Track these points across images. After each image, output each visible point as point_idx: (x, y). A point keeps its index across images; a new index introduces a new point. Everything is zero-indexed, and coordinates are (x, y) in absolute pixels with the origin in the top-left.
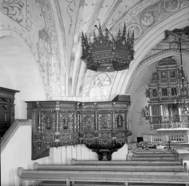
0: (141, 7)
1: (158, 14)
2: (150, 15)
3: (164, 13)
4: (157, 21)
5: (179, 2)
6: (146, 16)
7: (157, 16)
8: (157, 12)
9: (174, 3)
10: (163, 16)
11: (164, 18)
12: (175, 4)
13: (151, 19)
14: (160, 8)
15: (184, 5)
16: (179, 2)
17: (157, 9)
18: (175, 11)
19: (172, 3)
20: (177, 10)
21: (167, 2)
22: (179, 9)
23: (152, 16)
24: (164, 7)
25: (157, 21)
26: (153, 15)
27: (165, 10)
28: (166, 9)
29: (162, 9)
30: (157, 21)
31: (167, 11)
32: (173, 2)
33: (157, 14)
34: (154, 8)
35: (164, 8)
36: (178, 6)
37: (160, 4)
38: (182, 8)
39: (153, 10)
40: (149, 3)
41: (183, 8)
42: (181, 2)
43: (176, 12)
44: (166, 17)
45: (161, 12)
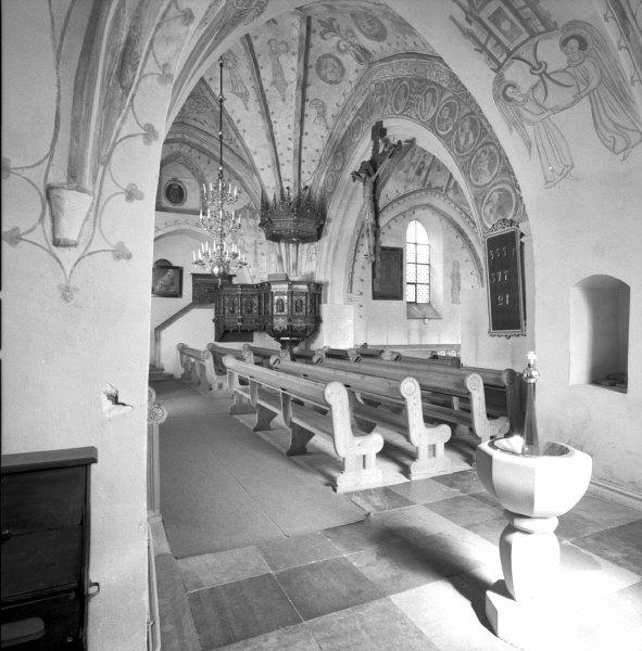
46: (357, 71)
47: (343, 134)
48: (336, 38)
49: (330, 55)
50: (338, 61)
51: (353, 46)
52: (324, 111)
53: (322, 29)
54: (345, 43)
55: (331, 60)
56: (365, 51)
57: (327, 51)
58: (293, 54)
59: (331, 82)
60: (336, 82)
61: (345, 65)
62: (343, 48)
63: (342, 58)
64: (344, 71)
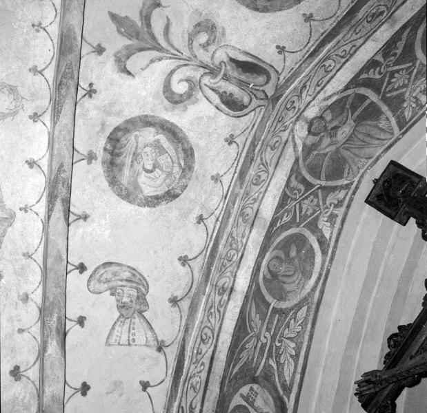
0: (191, 393)
1: (270, 355)
2: (245, 390)
3: (289, 323)
4: (287, 389)
5: (307, 233)
6: (238, 407)
7: (272, 363)
8: (264, 346)
9: (293, 254)
10: (291, 339)
11: (305, 344)
12: (299, 251)
13: (259, 403)
14: (262, 324)
15: (332, 218)
16: (307, 233)
17: (253, 341)
18: (320, 275)
19: (290, 260)
20: (324, 262)
21: (269, 276)
22: (324, 252)
23: (255, 386)
24: (273, 303)
25: (284, 386)
26: (254, 380)
27: (283, 313)
28: (284, 305)
29: (270, 322)
30: (284, 386)
31: (292, 309)
32: (287, 255)
33: (267, 359)
34: (243, 348)
35: (275, 310)
36: (316, 246)
37: (254, 309)
38: (333, 239)
39: (244, 356)
40: (204, 348)
41: (336, 231)
42: (313, 226)
43: (325, 276)
44: (307, 338)
45: (273, 338)
46: (230, 141)
47: (230, 324)
48: (165, 65)
49: (147, 122)
50: (173, 133)
51: (213, 72)
52: (141, 298)
53: (122, 42)
54: (187, 72)
55: (149, 135)
56: (251, 67)
57: (136, 112)
58: (35, 117)
59: (153, 201)
60: (171, 196)
61: (192, 137)
62: (180, 88)
63: (181, 119)
64: (189, 153)
